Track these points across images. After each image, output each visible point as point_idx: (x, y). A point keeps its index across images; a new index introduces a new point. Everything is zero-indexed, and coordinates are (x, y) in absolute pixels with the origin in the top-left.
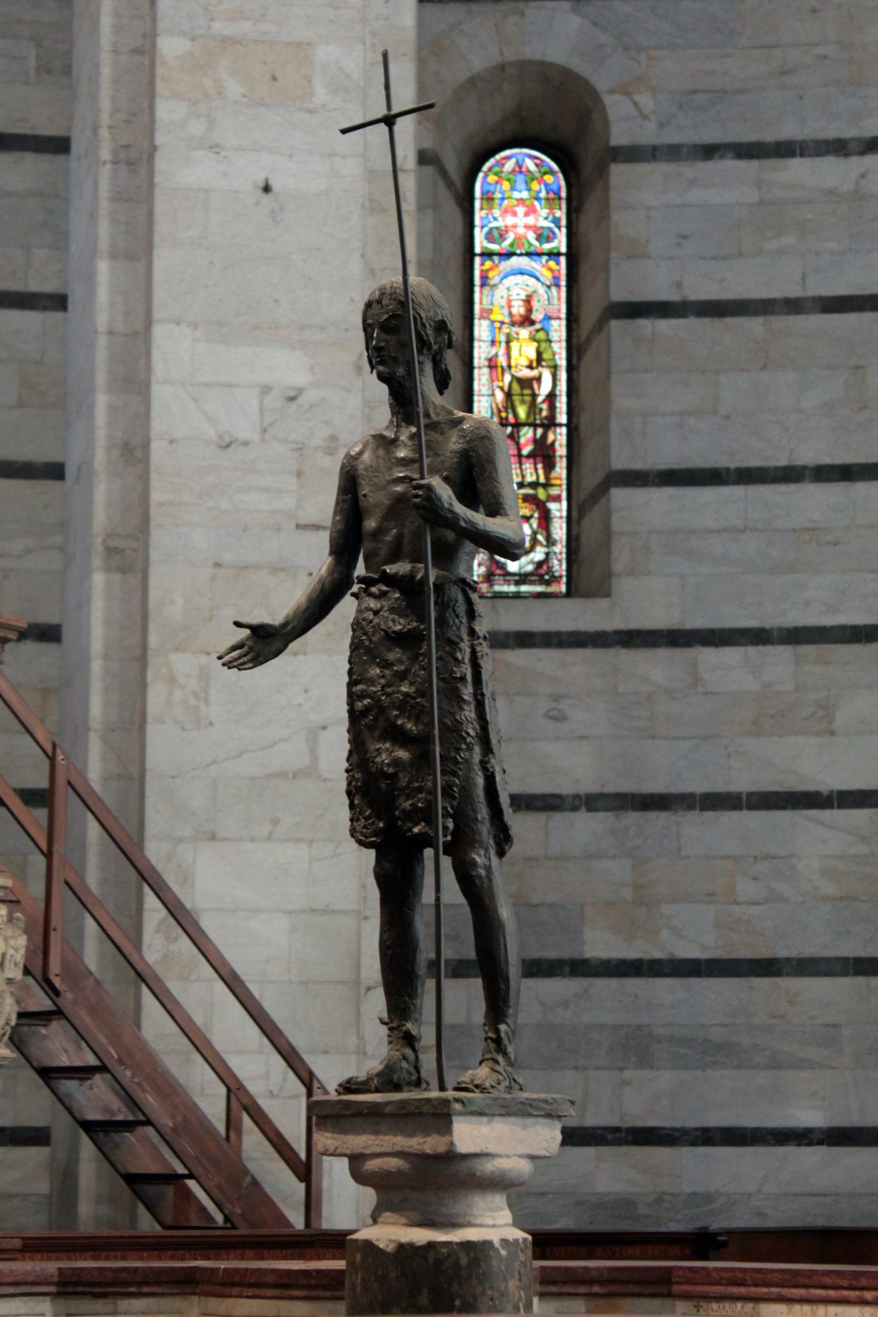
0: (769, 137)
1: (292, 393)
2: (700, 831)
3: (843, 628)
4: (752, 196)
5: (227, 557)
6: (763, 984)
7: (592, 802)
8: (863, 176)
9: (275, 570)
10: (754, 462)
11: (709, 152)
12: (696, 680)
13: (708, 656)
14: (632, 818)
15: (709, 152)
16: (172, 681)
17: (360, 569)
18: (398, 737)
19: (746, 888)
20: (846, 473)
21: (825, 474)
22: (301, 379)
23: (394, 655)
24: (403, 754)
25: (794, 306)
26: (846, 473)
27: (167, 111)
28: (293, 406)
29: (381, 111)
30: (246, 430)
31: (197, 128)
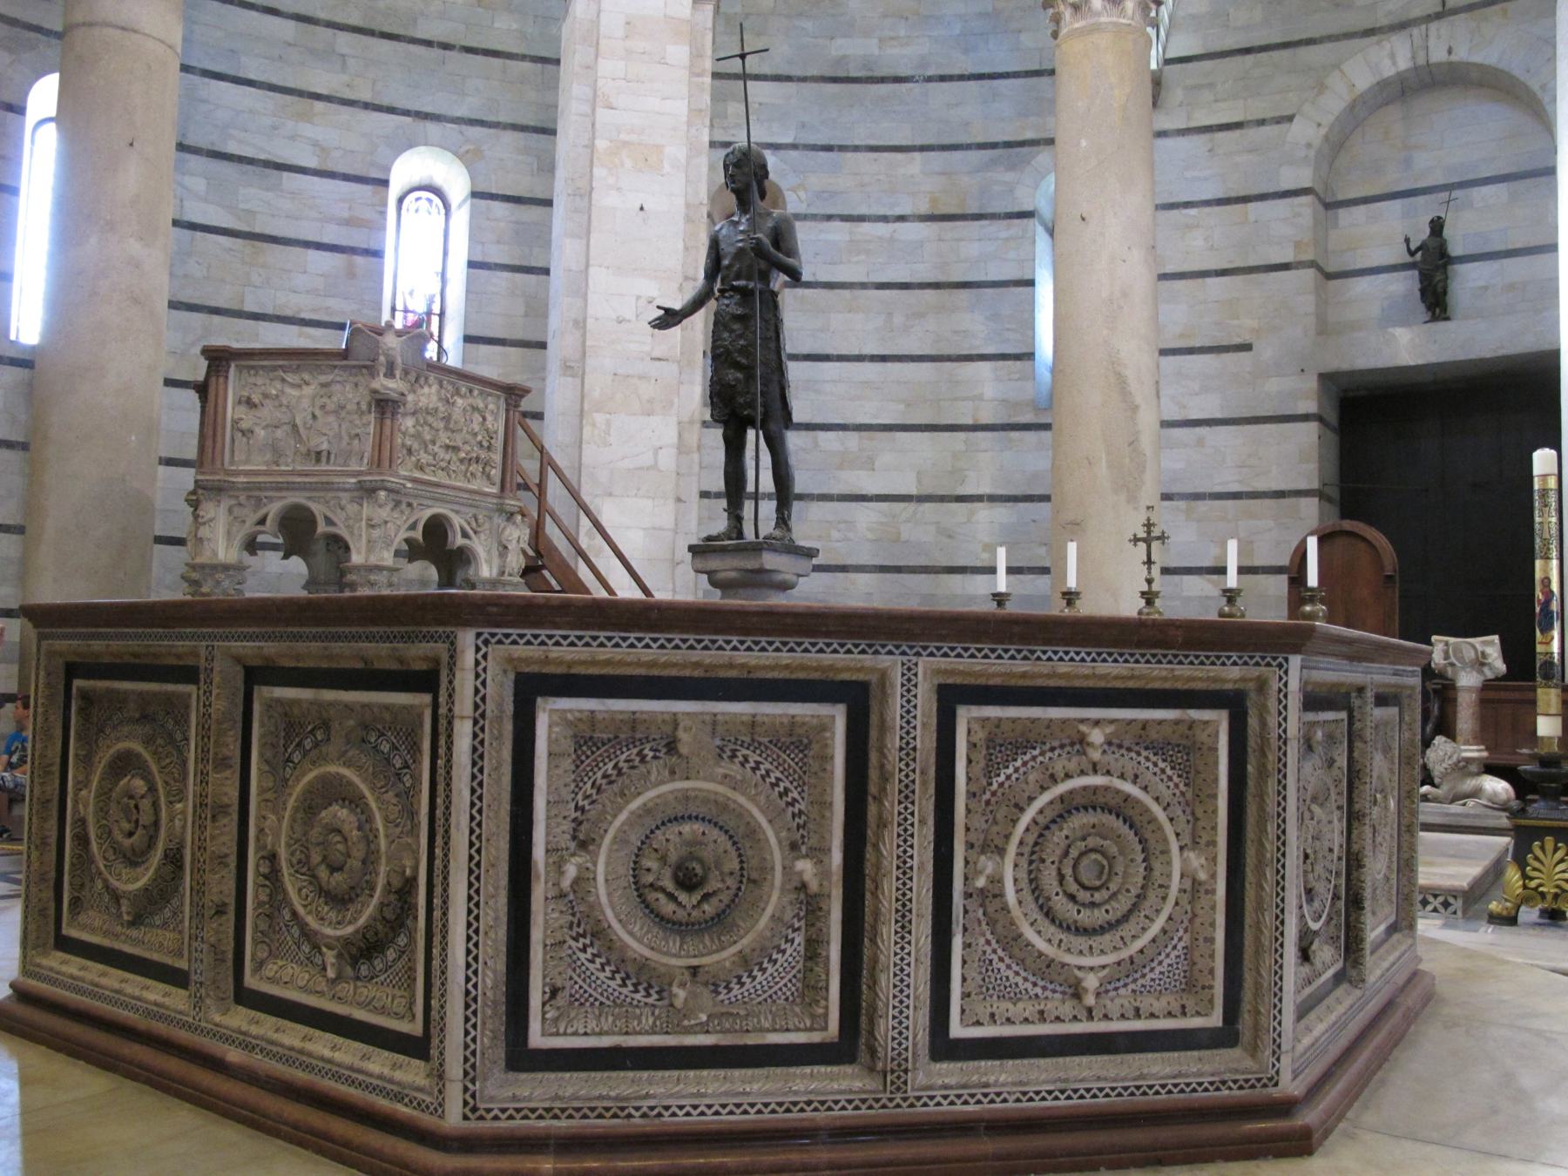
0: (855, 213)
5: (620, 371)
6: (841, 575)
9: (640, 378)
11: (829, 218)
12: (816, 445)
13: (821, 435)
15: (829, 218)
16: (594, 425)
17: (718, 285)
18: (737, 366)
19: (835, 534)
20: (883, 359)
21: (874, 358)
23: (736, 326)
24: (740, 375)
25: (864, 286)
26: (883, 359)
27: (598, 172)
29: (738, 52)
30: (629, 314)
31: (611, 181)
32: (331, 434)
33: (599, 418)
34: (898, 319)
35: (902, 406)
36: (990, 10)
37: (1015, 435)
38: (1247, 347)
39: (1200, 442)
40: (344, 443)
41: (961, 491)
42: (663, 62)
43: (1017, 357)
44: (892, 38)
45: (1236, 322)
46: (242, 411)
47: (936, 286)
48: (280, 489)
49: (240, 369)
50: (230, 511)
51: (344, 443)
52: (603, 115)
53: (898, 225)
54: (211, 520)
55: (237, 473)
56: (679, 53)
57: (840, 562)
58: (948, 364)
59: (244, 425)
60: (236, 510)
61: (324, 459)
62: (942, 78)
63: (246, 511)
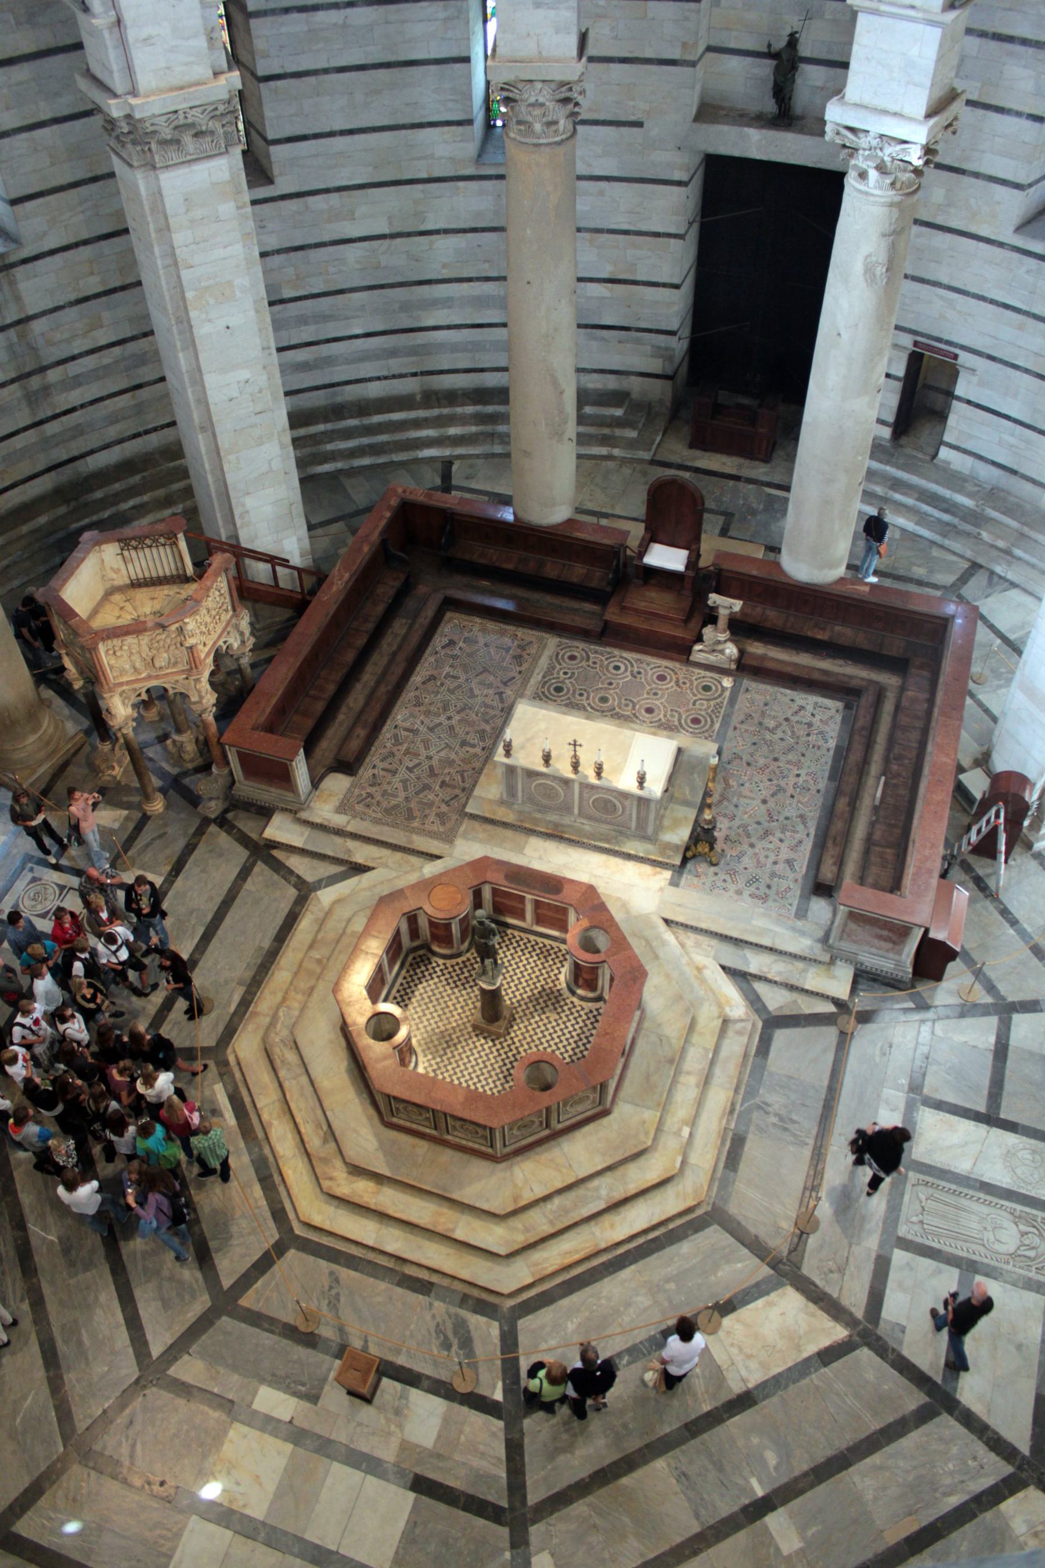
2: (314, 254)
4: (306, 28)
7: (279, 252)
10: (318, 131)
11: (287, 10)
12: (307, 208)
13: (310, 199)
14: (292, 254)
15: (287, 10)
19: (332, 270)
20: (351, 132)
21: (343, 133)
25: (326, 71)
26: (351, 132)
27: (193, 314)
30: (235, 394)
31: (203, 316)
33: (232, 457)
35: (371, 169)
37: (461, 184)
38: (639, 124)
39: (601, 193)
41: (423, 228)
42: (218, 220)
43: (459, 123)
45: (632, 103)
47: (388, 65)
56: (227, 208)
57: (339, 287)
58: (404, 132)
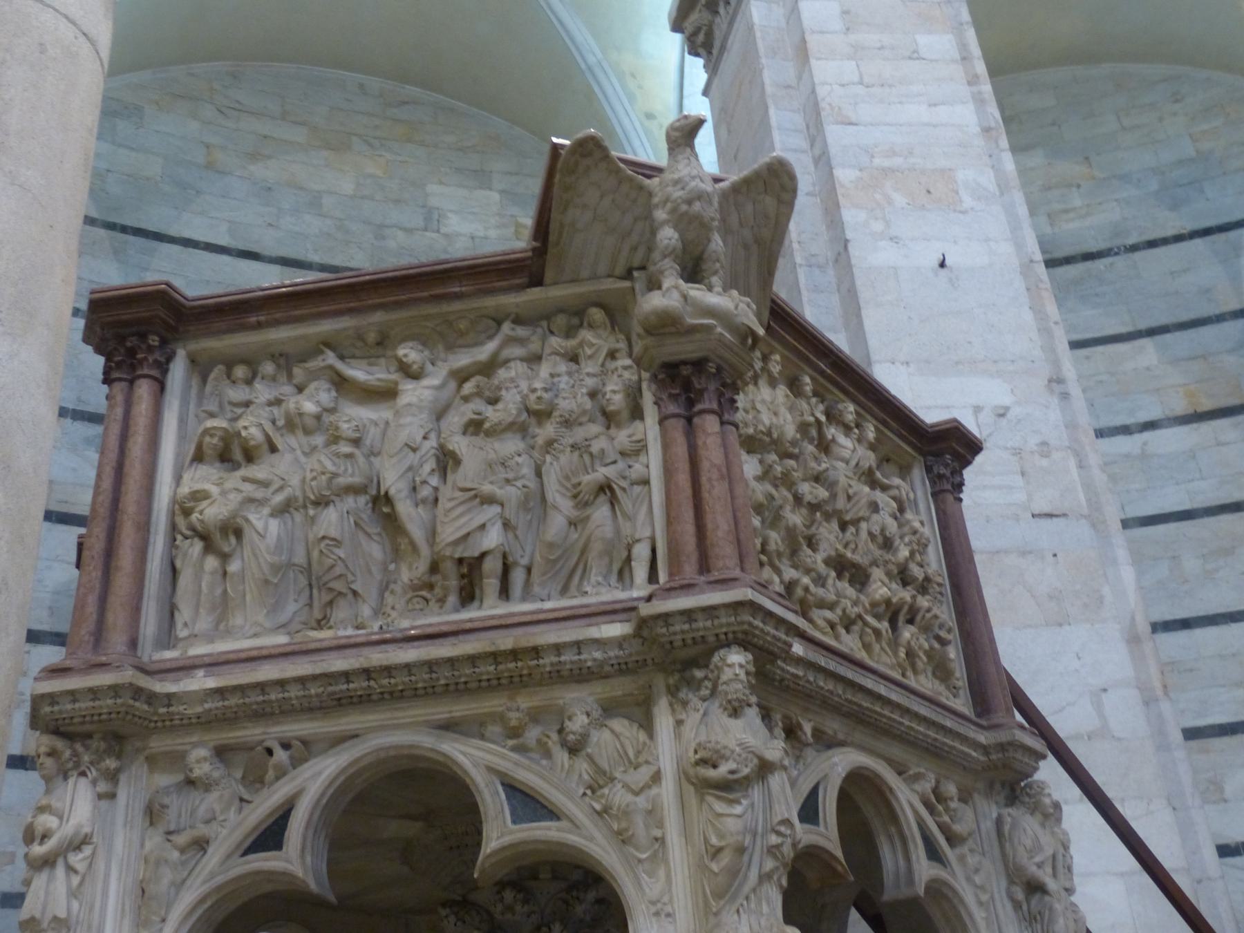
1: (1002, 411)
3: (1212, 727)
8: (1145, 444)
9: (1024, 553)
22: (1007, 400)
27: (850, 216)
28: (1004, 422)
31: (878, 226)
32: (511, 493)
34: (1191, 564)
36: (1193, 154)
40: (556, 525)
42: (915, 56)
44: (1066, 211)
46: (204, 477)
48: (344, 703)
49: (200, 368)
50: (153, 813)
51: (556, 525)
52: (836, 135)
53: (1147, 435)
54: (78, 843)
55: (186, 668)
59: (212, 513)
60: (178, 806)
61: (491, 584)
62: (1152, 244)
63: (210, 801)
